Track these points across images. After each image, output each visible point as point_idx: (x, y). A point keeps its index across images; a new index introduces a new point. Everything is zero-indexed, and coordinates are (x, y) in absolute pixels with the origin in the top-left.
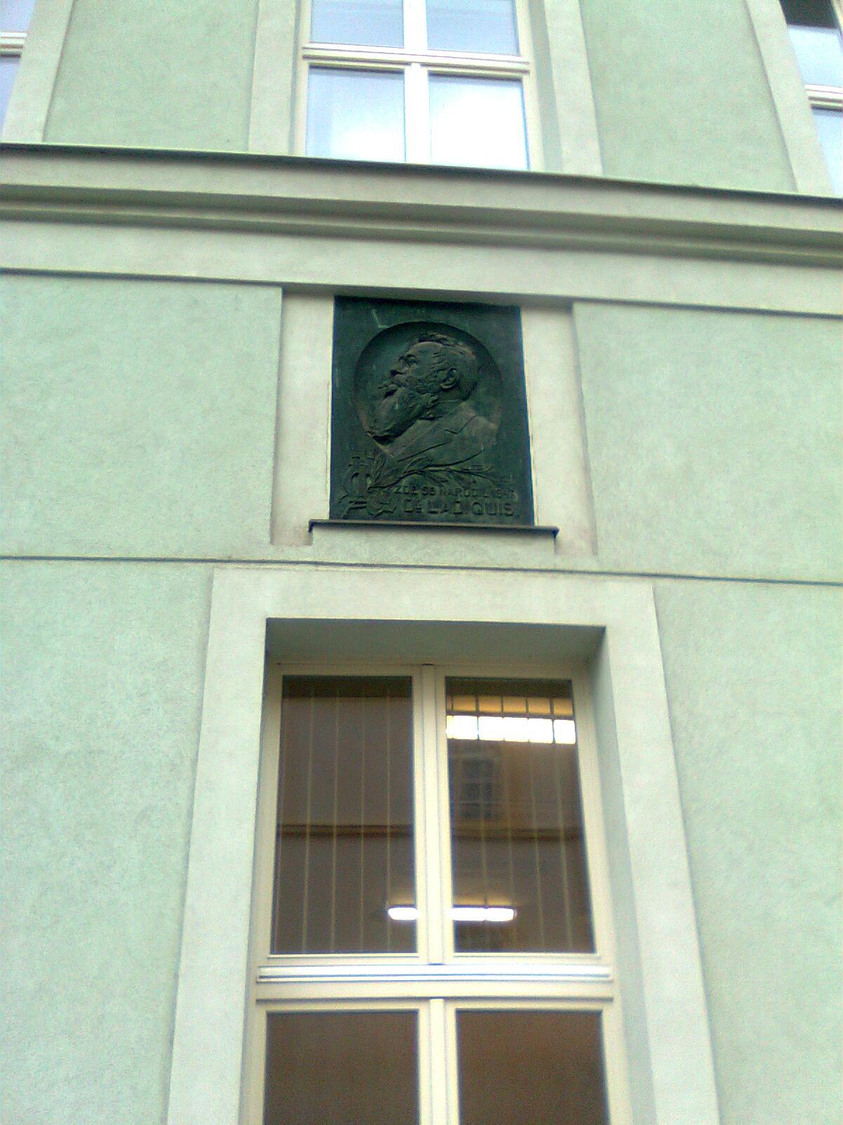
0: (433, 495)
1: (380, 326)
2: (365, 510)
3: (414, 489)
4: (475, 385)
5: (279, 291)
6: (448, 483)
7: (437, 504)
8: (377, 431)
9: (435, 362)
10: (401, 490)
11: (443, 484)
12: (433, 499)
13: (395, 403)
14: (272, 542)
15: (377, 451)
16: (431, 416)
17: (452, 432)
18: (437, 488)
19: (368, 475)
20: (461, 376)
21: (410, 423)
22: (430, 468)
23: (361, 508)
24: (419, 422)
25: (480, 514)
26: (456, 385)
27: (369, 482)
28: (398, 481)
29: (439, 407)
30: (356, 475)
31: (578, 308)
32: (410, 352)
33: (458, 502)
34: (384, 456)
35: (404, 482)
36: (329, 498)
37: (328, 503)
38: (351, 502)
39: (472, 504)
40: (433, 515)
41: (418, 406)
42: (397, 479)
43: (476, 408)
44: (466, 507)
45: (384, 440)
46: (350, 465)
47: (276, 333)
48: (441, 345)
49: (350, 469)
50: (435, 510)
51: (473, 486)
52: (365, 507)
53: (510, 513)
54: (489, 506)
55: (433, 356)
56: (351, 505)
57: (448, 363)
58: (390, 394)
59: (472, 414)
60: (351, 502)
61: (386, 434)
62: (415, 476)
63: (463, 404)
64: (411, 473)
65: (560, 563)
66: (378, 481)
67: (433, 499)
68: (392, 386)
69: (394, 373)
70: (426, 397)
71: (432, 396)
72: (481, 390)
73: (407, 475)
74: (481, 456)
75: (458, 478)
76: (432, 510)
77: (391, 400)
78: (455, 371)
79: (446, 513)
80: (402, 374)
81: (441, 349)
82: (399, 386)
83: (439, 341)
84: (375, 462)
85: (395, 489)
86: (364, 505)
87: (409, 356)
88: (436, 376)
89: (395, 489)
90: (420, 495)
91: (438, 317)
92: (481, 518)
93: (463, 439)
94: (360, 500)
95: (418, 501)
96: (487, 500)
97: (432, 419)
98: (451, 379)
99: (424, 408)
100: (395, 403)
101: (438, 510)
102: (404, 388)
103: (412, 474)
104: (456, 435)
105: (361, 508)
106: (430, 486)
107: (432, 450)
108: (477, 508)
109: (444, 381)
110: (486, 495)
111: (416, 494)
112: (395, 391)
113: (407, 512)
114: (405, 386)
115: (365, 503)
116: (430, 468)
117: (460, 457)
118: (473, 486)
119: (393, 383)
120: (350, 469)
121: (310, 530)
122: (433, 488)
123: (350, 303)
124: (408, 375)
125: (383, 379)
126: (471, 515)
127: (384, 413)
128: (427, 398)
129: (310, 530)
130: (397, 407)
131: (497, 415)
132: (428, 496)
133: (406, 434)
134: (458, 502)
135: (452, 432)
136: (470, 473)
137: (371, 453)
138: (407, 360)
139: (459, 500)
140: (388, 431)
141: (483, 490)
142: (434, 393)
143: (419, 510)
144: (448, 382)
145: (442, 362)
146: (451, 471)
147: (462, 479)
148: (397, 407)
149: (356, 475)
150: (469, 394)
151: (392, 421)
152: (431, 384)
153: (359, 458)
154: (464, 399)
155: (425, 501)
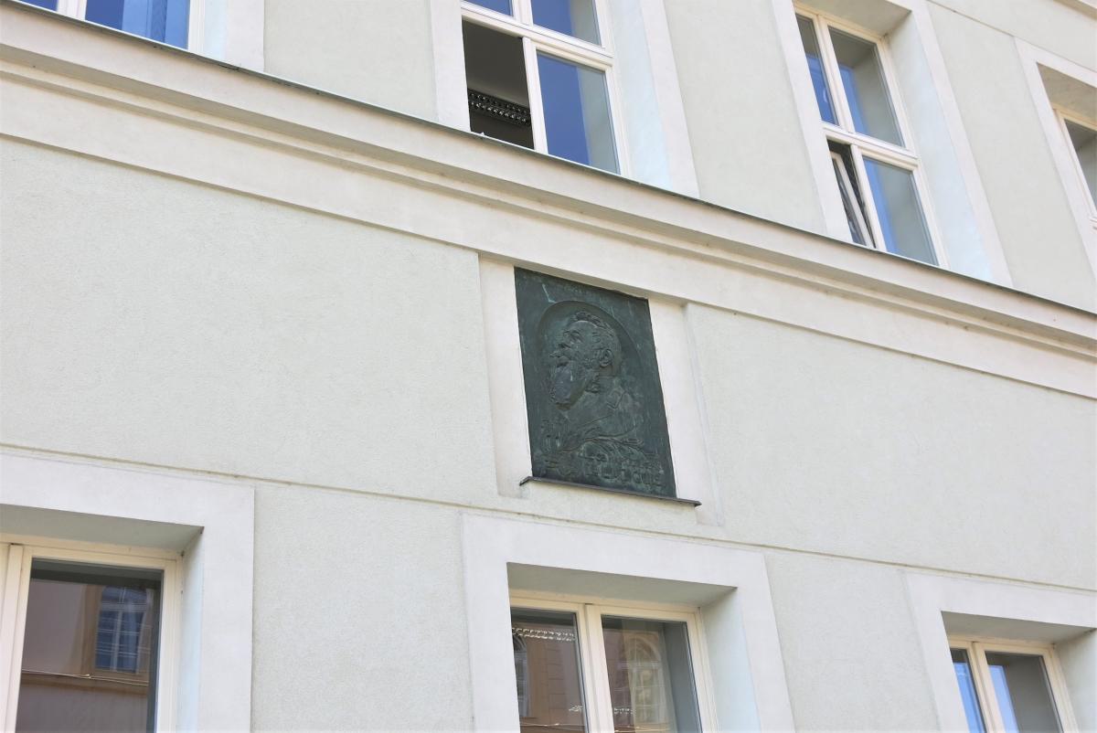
1: (550, 301)
3: (591, 454)
7: (608, 470)
16: (596, 390)
19: (557, 438)
21: (581, 394)
24: (586, 393)
30: (548, 436)
31: (690, 307)
40: (607, 481)
45: (566, 406)
48: (596, 327)
49: (542, 430)
54: (644, 476)
58: (563, 365)
61: (566, 402)
62: (590, 443)
65: (700, 531)
67: (605, 465)
69: (562, 346)
74: (634, 431)
75: (620, 449)
82: (570, 359)
83: (594, 321)
85: (577, 453)
87: (575, 332)
93: (620, 413)
97: (595, 392)
99: (591, 382)
106: (601, 453)
112: (567, 363)
114: (575, 359)
118: (632, 457)
120: (542, 430)
123: (530, 280)
128: (591, 373)
133: (578, 403)
138: (573, 336)
139: (623, 468)
141: (638, 461)
143: (596, 475)
146: (615, 442)
147: (624, 450)
149: (548, 436)
155: (600, 466)
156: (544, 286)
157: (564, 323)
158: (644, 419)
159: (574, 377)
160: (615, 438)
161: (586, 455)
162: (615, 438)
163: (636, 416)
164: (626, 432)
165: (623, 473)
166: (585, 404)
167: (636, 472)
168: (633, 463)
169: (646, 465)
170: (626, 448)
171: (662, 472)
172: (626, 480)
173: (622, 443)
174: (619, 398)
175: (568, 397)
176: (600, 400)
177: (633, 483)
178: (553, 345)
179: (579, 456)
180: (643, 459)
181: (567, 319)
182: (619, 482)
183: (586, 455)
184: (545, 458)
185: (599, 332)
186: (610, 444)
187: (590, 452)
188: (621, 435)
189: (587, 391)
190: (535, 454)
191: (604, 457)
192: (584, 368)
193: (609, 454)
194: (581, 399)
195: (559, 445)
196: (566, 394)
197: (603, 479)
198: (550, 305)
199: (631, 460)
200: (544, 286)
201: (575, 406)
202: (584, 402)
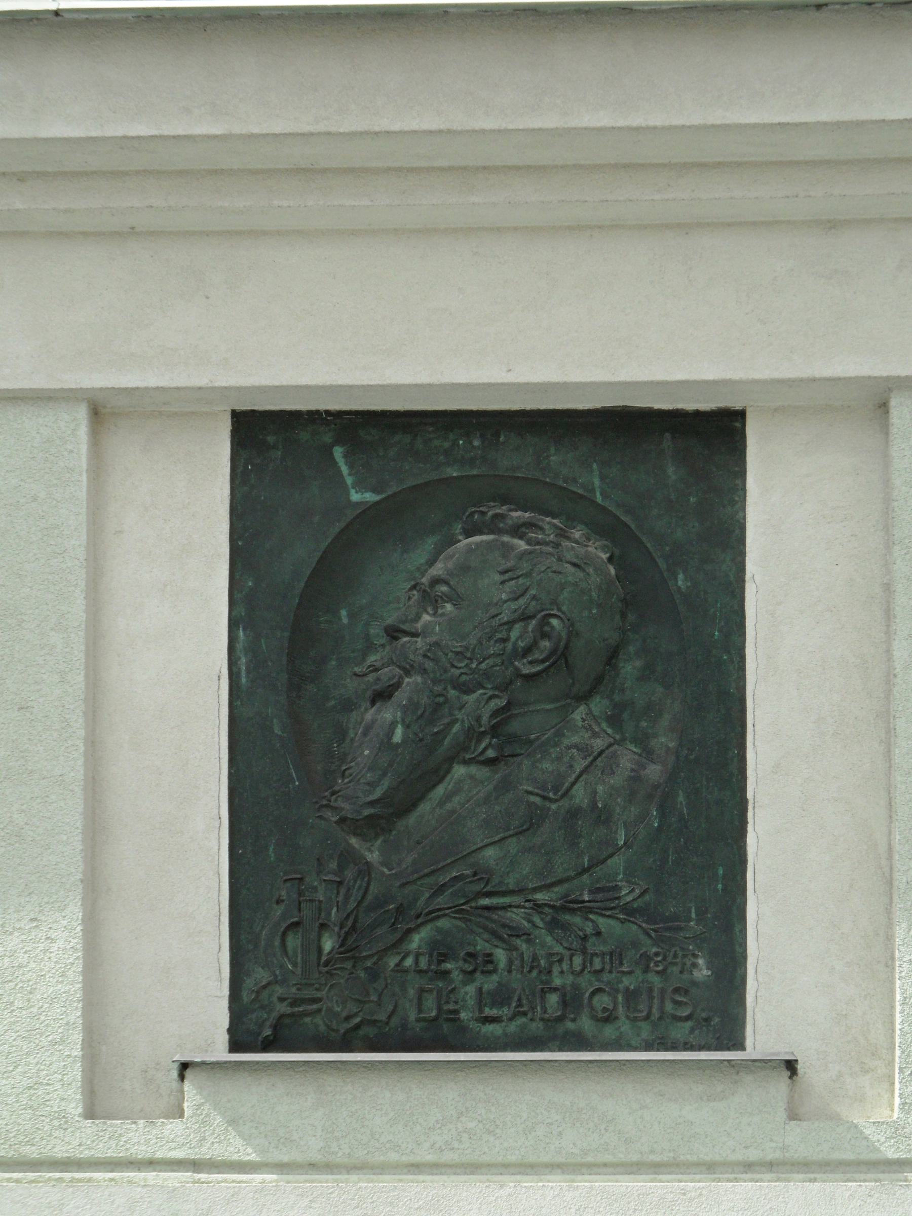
0: (490, 972)
1: (355, 497)
2: (318, 1020)
3: (443, 958)
4: (613, 655)
5: (82, 413)
6: (529, 941)
7: (500, 997)
8: (346, 806)
9: (504, 596)
10: (409, 962)
11: (518, 942)
12: (490, 983)
13: (393, 725)
14: (90, 1113)
15: (347, 857)
16: (491, 753)
17: (545, 798)
18: (501, 955)
19: (323, 926)
20: (573, 633)
21: (438, 774)
22: (486, 902)
23: (305, 1014)
24: (459, 771)
25: (609, 1018)
26: (561, 657)
27: (328, 945)
28: (401, 940)
29: (515, 726)
30: (297, 924)
31: (901, 410)
32: (438, 569)
33: (555, 989)
34: (366, 870)
35: (416, 941)
36: (226, 992)
37: (225, 1003)
38: (282, 1000)
39: (587, 995)
40: (489, 1028)
41: (456, 728)
42: (398, 935)
43: (614, 720)
44: (571, 1002)
46: (278, 902)
47: (77, 543)
48: (522, 545)
49: (278, 911)
50: (494, 1012)
51: (593, 946)
52: (319, 1011)
53: (685, 1012)
54: (631, 996)
55: (498, 578)
56: (283, 1008)
57: (534, 598)
58: (382, 695)
59: (599, 744)
60: (282, 1000)
61: (367, 812)
63: (579, 714)
64: (433, 915)
65: (797, 1140)
66: (350, 941)
67: (490, 983)
68: (388, 673)
69: (393, 633)
70: (478, 701)
71: (491, 698)
72: (629, 668)
73: (422, 924)
74: (617, 862)
75: (554, 925)
76: (488, 1012)
77: (388, 713)
78: (554, 622)
79: (524, 1020)
80: (415, 635)
81: (523, 555)
82: (408, 673)
83: (517, 531)
84: (343, 891)
85: (392, 962)
86: (315, 1007)
87: (436, 581)
88: (505, 640)
89: (392, 962)
90: (456, 976)
91: (514, 458)
92: (609, 1031)
93: (574, 814)
94: (308, 993)
95: (453, 990)
96: (626, 981)
98: (546, 644)
99: (472, 734)
100: (393, 725)
101: (505, 1011)
102: (419, 679)
103: (438, 917)
104: (554, 807)
105: (305, 1014)
106: (481, 945)
107: (490, 852)
108: (602, 1001)
109: (527, 651)
110: (625, 969)
111: (447, 972)
112: (397, 686)
113: (424, 1020)
115: (319, 1000)
116: (486, 902)
117: (562, 865)
119: (391, 662)
120: (278, 911)
121: (182, 1077)
122: (490, 955)
123: (267, 440)
124: (428, 640)
125: (370, 647)
126: (586, 1024)
127: (367, 752)
128: (479, 705)
129: (182, 1077)
130: (398, 735)
131: (664, 741)
132: (478, 975)
133: (424, 807)
134: (555, 989)
135: (545, 798)
136: (585, 910)
137: (333, 865)
138: (429, 598)
139: (557, 982)
140: (372, 803)
141: (616, 956)
142: (505, 687)
143: (453, 1017)
144: (537, 655)
145: (523, 595)
146: (538, 907)
147: (565, 927)
148: (398, 735)
150: (599, 680)
151: (384, 774)
152: (489, 662)
153: (301, 879)
154: (584, 697)
155: (471, 989)
156: (338, 452)
157: (419, 557)
158: (663, 815)
159: (407, 727)
160: (540, 897)
161: (423, 964)
162: (540, 897)
163: (634, 810)
164: (585, 871)
165: (553, 999)
166: (448, 806)
167: (599, 990)
168: (597, 964)
169: (645, 961)
170: (577, 920)
171: (703, 972)
172: (561, 1019)
173: (564, 909)
174: (580, 765)
175: (378, 793)
176: (505, 786)
177: (586, 1024)
178: (367, 637)
179: (399, 968)
180: (635, 944)
181: (430, 543)
182: (537, 1027)
183: (423, 963)
184: (279, 990)
185: (525, 566)
186: (516, 917)
187: (441, 951)
188: (560, 882)
189: (466, 762)
190: (249, 983)
191: (489, 959)
192: (452, 693)
193: (512, 948)
194: (440, 790)
195: (328, 945)
196: (372, 785)
197: (473, 1025)
198: (350, 514)
199: (589, 958)
200: (338, 452)
201: (412, 819)
202: (448, 797)
